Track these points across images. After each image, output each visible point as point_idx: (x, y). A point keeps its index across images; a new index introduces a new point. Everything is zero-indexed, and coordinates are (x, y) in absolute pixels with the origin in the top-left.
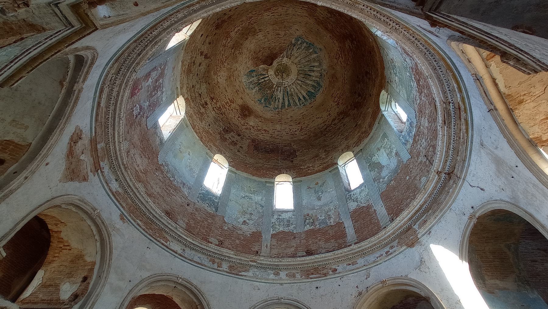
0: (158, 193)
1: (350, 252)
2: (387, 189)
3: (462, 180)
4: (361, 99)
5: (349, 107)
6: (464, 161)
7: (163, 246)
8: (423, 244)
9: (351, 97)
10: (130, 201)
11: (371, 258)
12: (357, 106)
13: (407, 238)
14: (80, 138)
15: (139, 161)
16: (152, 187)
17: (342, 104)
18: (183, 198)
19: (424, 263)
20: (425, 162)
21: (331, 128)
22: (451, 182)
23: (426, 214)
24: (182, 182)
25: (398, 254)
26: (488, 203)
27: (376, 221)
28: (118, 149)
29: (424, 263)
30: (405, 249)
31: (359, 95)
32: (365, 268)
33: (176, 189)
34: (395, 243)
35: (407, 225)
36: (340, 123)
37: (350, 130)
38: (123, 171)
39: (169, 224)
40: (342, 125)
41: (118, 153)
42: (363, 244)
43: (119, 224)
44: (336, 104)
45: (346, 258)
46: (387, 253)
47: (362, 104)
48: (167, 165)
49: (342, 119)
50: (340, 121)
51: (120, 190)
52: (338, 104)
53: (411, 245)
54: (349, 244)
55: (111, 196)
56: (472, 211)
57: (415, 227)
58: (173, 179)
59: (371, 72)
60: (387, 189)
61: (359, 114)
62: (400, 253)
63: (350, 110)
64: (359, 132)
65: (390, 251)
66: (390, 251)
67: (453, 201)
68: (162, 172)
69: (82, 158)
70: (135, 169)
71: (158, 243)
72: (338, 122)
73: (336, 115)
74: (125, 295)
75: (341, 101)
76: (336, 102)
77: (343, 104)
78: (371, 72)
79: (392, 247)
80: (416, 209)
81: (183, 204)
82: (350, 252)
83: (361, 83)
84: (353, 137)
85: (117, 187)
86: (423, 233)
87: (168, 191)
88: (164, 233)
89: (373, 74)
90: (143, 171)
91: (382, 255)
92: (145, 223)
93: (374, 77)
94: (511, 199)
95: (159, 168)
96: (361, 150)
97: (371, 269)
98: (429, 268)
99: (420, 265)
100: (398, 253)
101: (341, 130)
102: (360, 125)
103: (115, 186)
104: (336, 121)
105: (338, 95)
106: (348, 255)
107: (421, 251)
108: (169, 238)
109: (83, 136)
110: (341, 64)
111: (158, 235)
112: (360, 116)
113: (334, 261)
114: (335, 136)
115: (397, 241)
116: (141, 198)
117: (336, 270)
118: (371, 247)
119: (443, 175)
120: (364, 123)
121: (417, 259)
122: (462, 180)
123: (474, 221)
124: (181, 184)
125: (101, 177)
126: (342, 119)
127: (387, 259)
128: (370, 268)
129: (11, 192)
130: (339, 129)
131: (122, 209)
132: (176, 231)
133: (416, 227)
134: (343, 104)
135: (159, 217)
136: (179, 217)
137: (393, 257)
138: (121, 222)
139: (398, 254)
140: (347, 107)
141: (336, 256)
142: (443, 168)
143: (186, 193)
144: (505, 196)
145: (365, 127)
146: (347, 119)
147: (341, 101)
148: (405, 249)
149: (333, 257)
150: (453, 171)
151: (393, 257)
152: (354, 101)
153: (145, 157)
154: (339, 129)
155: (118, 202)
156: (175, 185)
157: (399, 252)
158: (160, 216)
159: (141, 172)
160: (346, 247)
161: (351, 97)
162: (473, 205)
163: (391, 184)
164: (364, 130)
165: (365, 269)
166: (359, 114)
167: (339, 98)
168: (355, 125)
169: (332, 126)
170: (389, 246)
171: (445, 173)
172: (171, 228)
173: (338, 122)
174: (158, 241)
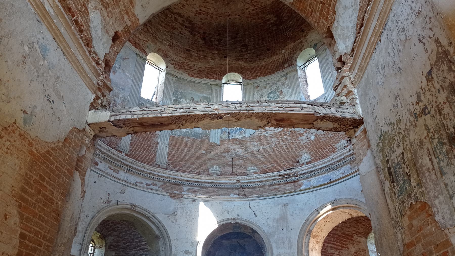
1: (122, 160)
2: (179, 139)
3: (247, 199)
4: (216, 45)
5: (201, 31)
6: (263, 196)
8: (183, 203)
9: (213, 29)
11: (132, 179)
12: (208, 43)
13: (172, 188)
17: (201, 19)
19: (175, 215)
20: (228, 161)
21: (170, 16)
22: (237, 191)
23: (200, 188)
25: (157, 194)
26: (253, 224)
27: (153, 153)
29: (175, 215)
30: (166, 195)
31: (219, 41)
32: (124, 183)
34: (159, 184)
35: (181, 181)
36: (181, 26)
37: (180, 45)
40: (180, 30)
42: (138, 164)
44: (199, 11)
45: (114, 161)
46: (147, 185)
47: (212, 48)
49: (186, 27)
50: (182, 25)
52: (199, 14)
53: (173, 196)
54: (120, 149)
56: (236, 217)
57: (184, 187)
59: (249, 52)
60: (179, 139)
61: (201, 49)
62: (159, 194)
63: (199, 33)
64: (184, 58)
65: (151, 186)
66: (151, 186)
67: (227, 201)
72: (179, 23)
73: (186, 16)
75: (203, 16)
76: (200, 10)
77: (201, 20)
78: (249, 52)
79: (154, 184)
80: (200, 180)
82: (122, 160)
83: (233, 40)
84: (177, 54)
86: (189, 197)
89: (248, 55)
91: (142, 183)
93: (245, 57)
94: (268, 233)
96: (177, 77)
97: (128, 187)
98: (176, 221)
99: (171, 215)
100: (158, 193)
101: (174, 31)
102: (192, 55)
104: (180, 19)
105: (209, 11)
106: (118, 160)
107: (178, 206)
110: (247, 9)
112: (200, 51)
113: (102, 155)
114: (165, 27)
115: (162, 183)
117: (98, 164)
118: (139, 170)
119: (238, 184)
120: (196, 60)
121: (172, 208)
122: (247, 199)
123: (233, 222)
126: (186, 27)
127: (147, 190)
128: (128, 186)
130: (174, 28)
133: (185, 188)
134: (201, 20)
137: (151, 192)
139: (157, 194)
140: (200, 28)
141: (109, 153)
142: (243, 183)
144: (266, 229)
145: (194, 65)
146: (186, 32)
147: (203, 16)
148: (166, 195)
149: (105, 151)
150: (244, 189)
151: (151, 192)
152: (210, 36)
154: (174, 28)
157: (160, 193)
160: (115, 149)
161: (213, 29)
162: (240, 214)
163: (185, 139)
164: (191, 64)
165: (123, 184)
166: (201, 49)
167: (206, 13)
168: (188, 48)
169: (172, 16)
170: (152, 181)
171: (240, 185)
173: (179, 23)
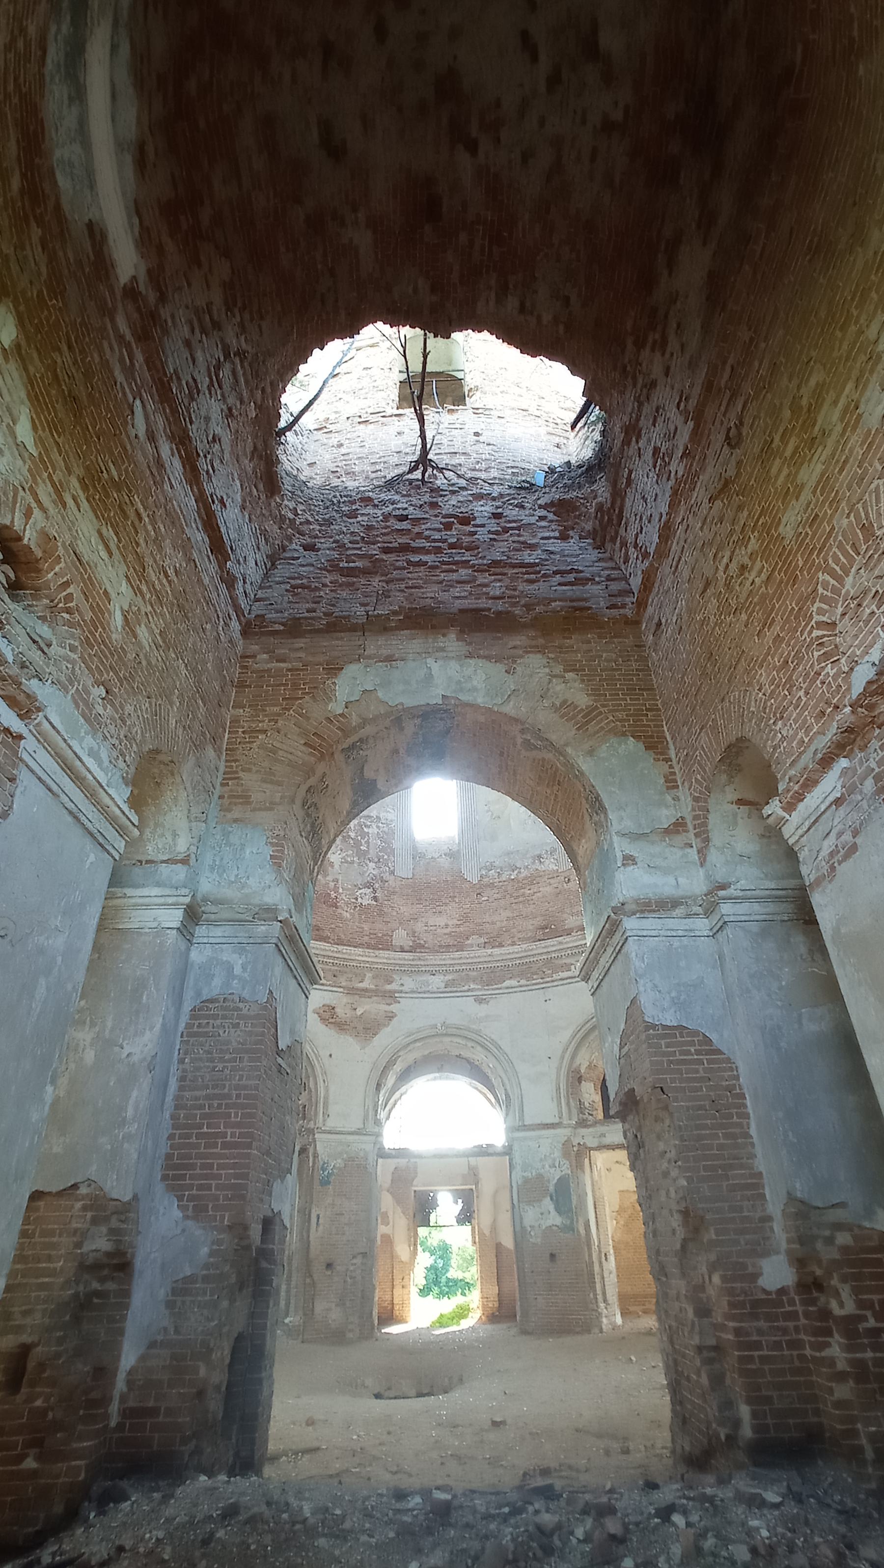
0: (508, 918)
7: (565, 982)
10: (475, 973)
14: (333, 1008)
15: (441, 921)
16: (493, 923)
18: (552, 881)
24: (533, 858)
28: (385, 961)
33: (533, 880)
38: (422, 963)
39: (545, 947)
41: (392, 961)
43: (482, 1010)
48: (491, 867)
51: (450, 977)
55: (442, 995)
58: (516, 872)
68: (491, 885)
69: (359, 1012)
70: (445, 934)
71: (555, 983)
74: (554, 1077)
81: (558, 891)
85: (442, 977)
87: (521, 899)
88: (556, 962)
90: (459, 923)
92: (521, 975)
95: (479, 889)
103: (437, 981)
108: (568, 961)
109: (333, 1003)
111: (550, 972)
116: (478, 960)
124: (533, 863)
125: (407, 995)
129: (326, 1098)
131: (469, 994)
132: (565, 946)
135: (525, 954)
136: (565, 916)
138: (484, 1006)
143: (553, 867)
153: (446, 904)
155: (456, 992)
156: (526, 878)
158: (525, 951)
159: (458, 926)
172: (554, 949)
174: (553, 981)
